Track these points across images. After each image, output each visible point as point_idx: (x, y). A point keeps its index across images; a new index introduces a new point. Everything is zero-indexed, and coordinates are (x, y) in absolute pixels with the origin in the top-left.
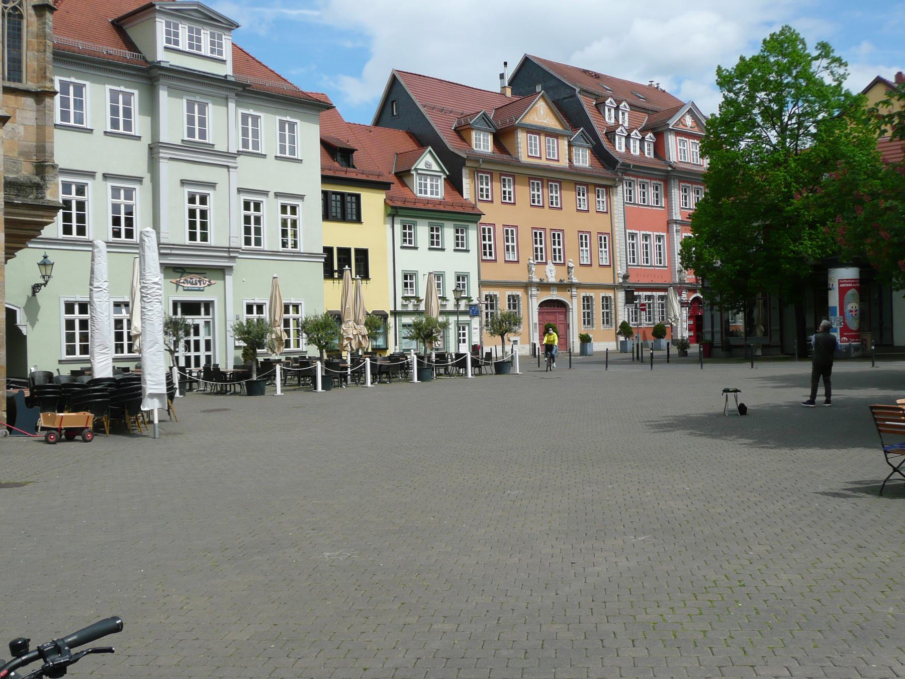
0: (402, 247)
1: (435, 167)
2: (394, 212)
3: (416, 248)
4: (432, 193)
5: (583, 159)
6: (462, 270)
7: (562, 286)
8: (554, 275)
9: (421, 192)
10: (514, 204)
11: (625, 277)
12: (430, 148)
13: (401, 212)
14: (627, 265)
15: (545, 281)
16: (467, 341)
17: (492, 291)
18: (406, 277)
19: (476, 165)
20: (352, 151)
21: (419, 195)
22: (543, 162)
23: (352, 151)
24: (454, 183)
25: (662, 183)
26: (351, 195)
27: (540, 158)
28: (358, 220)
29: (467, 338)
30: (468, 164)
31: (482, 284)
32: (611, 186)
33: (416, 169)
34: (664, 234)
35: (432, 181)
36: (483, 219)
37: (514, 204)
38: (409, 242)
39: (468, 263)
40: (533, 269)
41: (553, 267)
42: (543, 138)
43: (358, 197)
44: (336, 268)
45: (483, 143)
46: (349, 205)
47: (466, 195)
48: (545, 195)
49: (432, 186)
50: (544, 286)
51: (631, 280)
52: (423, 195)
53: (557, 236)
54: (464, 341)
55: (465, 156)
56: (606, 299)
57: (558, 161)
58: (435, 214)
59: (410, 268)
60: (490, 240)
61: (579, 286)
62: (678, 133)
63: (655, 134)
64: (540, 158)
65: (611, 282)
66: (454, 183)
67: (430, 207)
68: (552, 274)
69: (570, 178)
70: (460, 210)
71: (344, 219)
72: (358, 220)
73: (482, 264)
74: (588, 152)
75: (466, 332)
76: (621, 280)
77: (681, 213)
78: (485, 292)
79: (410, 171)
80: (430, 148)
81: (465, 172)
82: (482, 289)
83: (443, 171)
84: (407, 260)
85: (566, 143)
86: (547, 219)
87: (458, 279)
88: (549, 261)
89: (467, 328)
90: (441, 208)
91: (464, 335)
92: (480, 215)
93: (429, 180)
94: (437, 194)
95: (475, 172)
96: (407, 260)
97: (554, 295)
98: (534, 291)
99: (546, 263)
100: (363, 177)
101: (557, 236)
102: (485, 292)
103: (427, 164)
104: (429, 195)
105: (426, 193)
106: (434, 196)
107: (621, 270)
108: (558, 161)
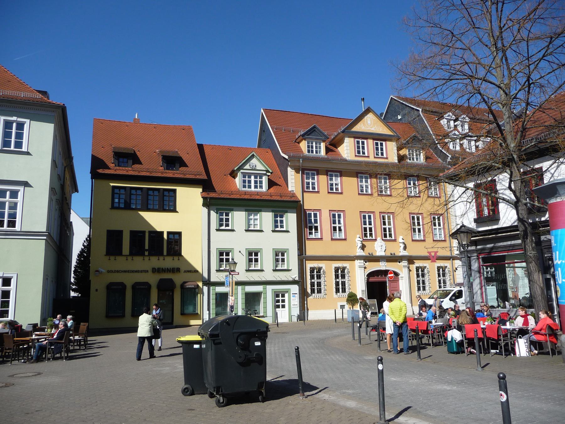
0: (217, 230)
3: (232, 230)
4: (256, 187)
16: (287, 306)
18: (221, 254)
27: (368, 157)
29: (286, 303)
35: (256, 177)
43: (175, 191)
44: (147, 247)
48: (369, 184)
49: (256, 182)
54: (283, 306)
57: (387, 158)
59: (225, 246)
68: (379, 248)
69: (402, 172)
84: (221, 240)
86: (377, 205)
88: (379, 239)
89: (286, 295)
91: (283, 301)
93: (253, 177)
94: (261, 187)
96: (221, 240)
97: (382, 266)
99: (376, 240)
105: (250, 187)
106: (258, 190)
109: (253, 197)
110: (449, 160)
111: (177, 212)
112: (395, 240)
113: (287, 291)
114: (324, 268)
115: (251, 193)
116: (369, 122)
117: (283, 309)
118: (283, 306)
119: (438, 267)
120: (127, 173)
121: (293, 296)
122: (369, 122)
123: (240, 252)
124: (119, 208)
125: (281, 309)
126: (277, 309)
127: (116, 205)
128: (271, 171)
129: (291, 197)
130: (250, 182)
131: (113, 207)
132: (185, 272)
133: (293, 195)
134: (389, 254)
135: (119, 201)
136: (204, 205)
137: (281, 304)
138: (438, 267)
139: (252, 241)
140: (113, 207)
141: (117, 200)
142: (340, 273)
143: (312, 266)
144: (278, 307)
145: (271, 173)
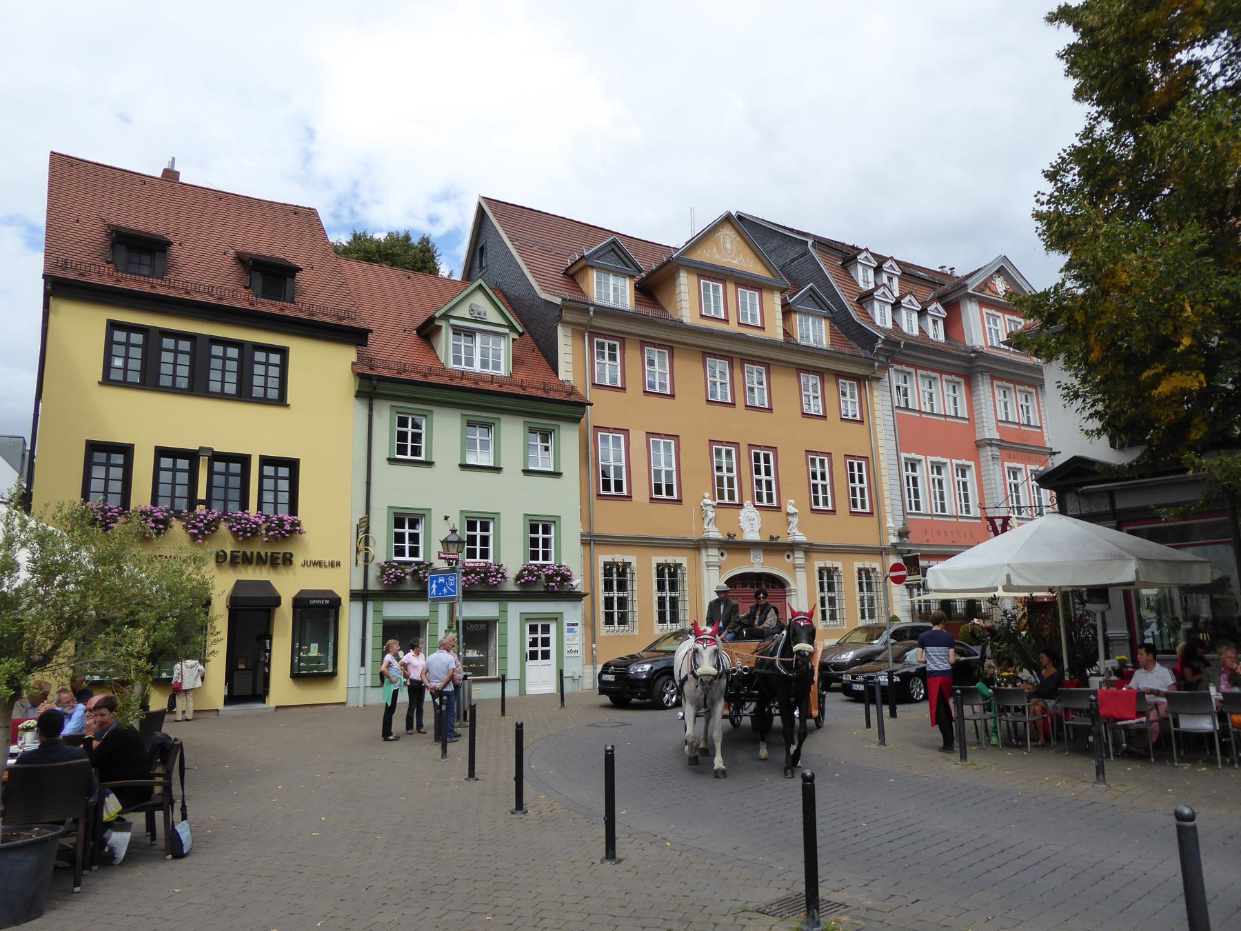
0: (391, 461)
1: (493, 316)
3: (429, 464)
4: (484, 364)
5: (815, 332)
6: (542, 509)
7: (773, 547)
8: (757, 527)
9: (457, 360)
11: (902, 534)
14: (905, 514)
15: (737, 539)
16: (553, 654)
19: (584, 320)
20: (292, 271)
21: (451, 365)
22: (732, 327)
23: (292, 271)
25: (962, 380)
27: (726, 321)
28: (281, 401)
29: (552, 648)
30: (567, 316)
31: (590, 541)
32: (866, 378)
34: (972, 463)
36: (593, 416)
39: (562, 500)
40: (711, 515)
41: (755, 514)
42: (731, 287)
43: (283, 352)
45: (615, 291)
50: (732, 546)
51: (913, 539)
52: (463, 367)
53: (762, 458)
54: (546, 655)
55: (558, 301)
56: (865, 573)
57: (762, 328)
58: (480, 401)
61: (809, 549)
62: (984, 303)
63: (945, 306)
64: (726, 321)
65: (873, 542)
68: (751, 525)
70: (540, 393)
71: (244, 394)
72: (281, 401)
74: (824, 325)
75: (552, 635)
76: (894, 539)
77: (999, 429)
78: (604, 557)
81: (561, 331)
82: (596, 549)
83: (512, 327)
84: (400, 487)
85: (777, 299)
87: (534, 529)
88: (747, 503)
89: (553, 627)
91: (546, 642)
92: (583, 405)
94: (497, 366)
96: (400, 487)
97: (757, 564)
98: (713, 555)
99: (741, 506)
101: (762, 458)
102: (604, 557)
104: (477, 367)
105: (470, 362)
106: (490, 371)
107: (893, 522)
108: (762, 328)
109: (481, 386)
110: (879, 345)
111: (287, 406)
112: (779, 508)
113: (557, 618)
114: (634, 565)
115: (477, 378)
116: (728, 246)
117: (545, 662)
118: (546, 655)
120: (154, 291)
121: (569, 631)
122: (728, 246)
124: (124, 384)
125: (540, 661)
126: (530, 662)
127: (116, 375)
129: (570, 394)
130: (470, 350)
131: (107, 381)
132: (305, 564)
133: (572, 391)
134: (767, 539)
135: (126, 363)
136: (359, 395)
137: (540, 648)
139: (478, 494)
140: (107, 381)
141: (118, 362)
142: (668, 577)
143: (609, 559)
144: (533, 656)
145: (521, 334)
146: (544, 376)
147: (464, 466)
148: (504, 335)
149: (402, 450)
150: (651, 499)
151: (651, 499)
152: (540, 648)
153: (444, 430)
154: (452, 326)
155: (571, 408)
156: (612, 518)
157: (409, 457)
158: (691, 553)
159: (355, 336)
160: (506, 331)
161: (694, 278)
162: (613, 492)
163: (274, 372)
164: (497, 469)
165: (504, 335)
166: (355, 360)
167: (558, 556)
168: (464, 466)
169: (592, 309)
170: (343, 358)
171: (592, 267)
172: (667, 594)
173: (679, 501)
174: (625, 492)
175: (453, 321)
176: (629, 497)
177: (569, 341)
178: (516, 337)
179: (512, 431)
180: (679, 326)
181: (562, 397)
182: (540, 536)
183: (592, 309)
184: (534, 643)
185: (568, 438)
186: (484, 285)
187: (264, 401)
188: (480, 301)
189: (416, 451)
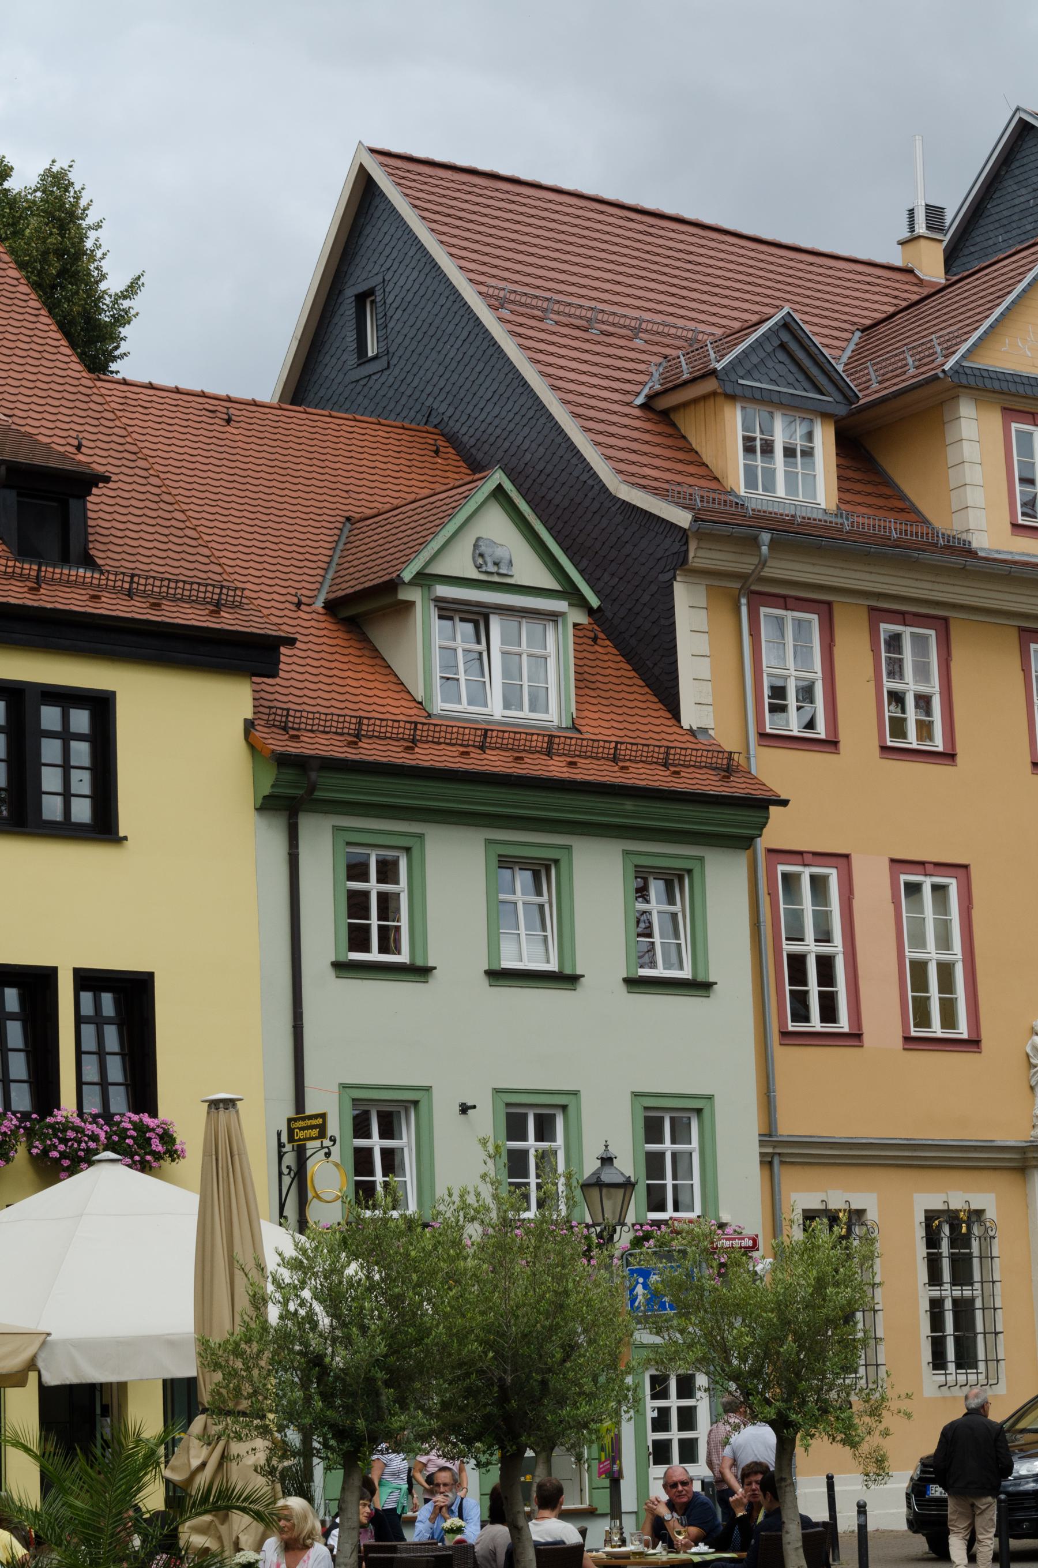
0: (342, 968)
1: (529, 570)
2: (296, 786)
3: (419, 972)
10: (949, 756)
12: (498, 477)
13: (330, 786)
17: (838, 1194)
19: (745, 564)
20: (85, 482)
23: (85, 482)
24: (634, 646)
26: (66, 698)
28: (104, 827)
30: (697, 555)
31: (779, 1154)
33: (425, 579)
36: (779, 830)
37: (949, 756)
38: (374, 940)
43: (101, 706)
46: (50, 750)
47: (691, 716)
55: (682, 518)
58: (523, 802)
59: (386, 1071)
60: (824, 937)
66: (634, 646)
67: (495, 762)
70: (658, 778)
72: (104, 827)
73: (786, 1057)
78: (804, 1194)
79: (392, 586)
80: (498, 477)
82: (787, 1177)
83: (571, 593)
84: (365, 1036)
90: (556, 768)
92: (761, 804)
95: (750, 595)
96: (365, 1036)
100: (136, 610)
102: (804, 1194)
103: (478, 554)
104: (496, 709)
106: (524, 714)
119: (930, 1216)
123: (464, 1109)
128: (594, 602)
137: (675, 1435)
138: (930, 1216)
145: (591, 611)
146: (644, 719)
147: (498, 976)
148: (554, 617)
149: (358, 939)
150: (908, 1039)
151: (908, 1039)
152: (675, 1435)
153: (452, 880)
154: (438, 600)
155: (733, 815)
156: (827, 1094)
157: (374, 956)
158: (1004, 1182)
159: (246, 655)
160: (560, 605)
161: (994, 419)
162: (816, 1024)
163: (81, 752)
164: (565, 979)
165: (554, 617)
166: (250, 716)
167: (710, 1198)
168: (498, 976)
169: (766, 537)
170: (222, 705)
171: (732, 398)
172: (948, 1292)
173: (973, 1043)
174: (844, 1024)
175: (443, 591)
176: (855, 1037)
177: (701, 620)
178: (582, 618)
179: (598, 876)
180: (959, 557)
181: (709, 784)
182: (667, 1146)
183: (766, 537)
184: (661, 1422)
185: (725, 886)
186: (508, 486)
187: (66, 831)
188: (497, 529)
189: (388, 941)
